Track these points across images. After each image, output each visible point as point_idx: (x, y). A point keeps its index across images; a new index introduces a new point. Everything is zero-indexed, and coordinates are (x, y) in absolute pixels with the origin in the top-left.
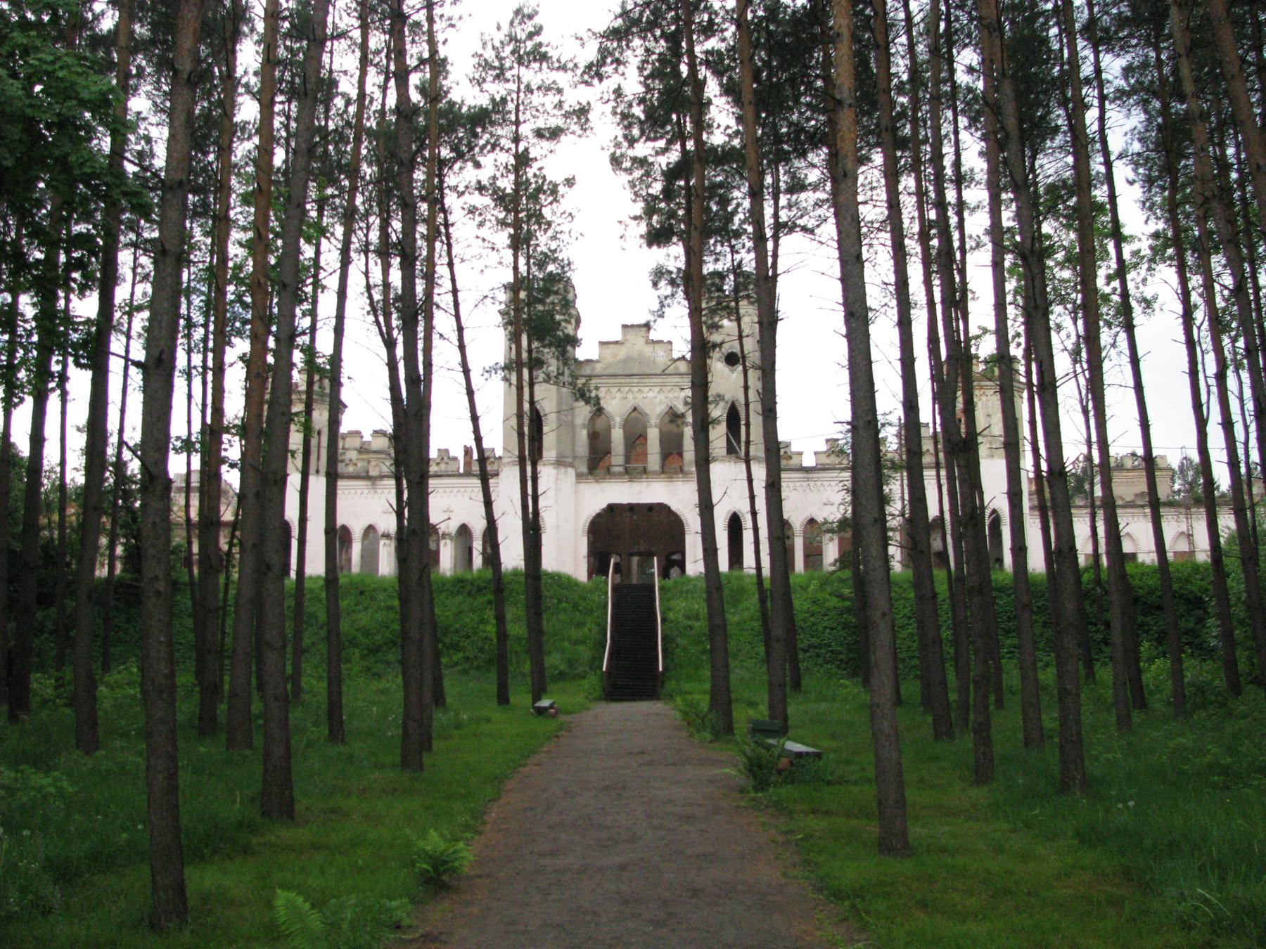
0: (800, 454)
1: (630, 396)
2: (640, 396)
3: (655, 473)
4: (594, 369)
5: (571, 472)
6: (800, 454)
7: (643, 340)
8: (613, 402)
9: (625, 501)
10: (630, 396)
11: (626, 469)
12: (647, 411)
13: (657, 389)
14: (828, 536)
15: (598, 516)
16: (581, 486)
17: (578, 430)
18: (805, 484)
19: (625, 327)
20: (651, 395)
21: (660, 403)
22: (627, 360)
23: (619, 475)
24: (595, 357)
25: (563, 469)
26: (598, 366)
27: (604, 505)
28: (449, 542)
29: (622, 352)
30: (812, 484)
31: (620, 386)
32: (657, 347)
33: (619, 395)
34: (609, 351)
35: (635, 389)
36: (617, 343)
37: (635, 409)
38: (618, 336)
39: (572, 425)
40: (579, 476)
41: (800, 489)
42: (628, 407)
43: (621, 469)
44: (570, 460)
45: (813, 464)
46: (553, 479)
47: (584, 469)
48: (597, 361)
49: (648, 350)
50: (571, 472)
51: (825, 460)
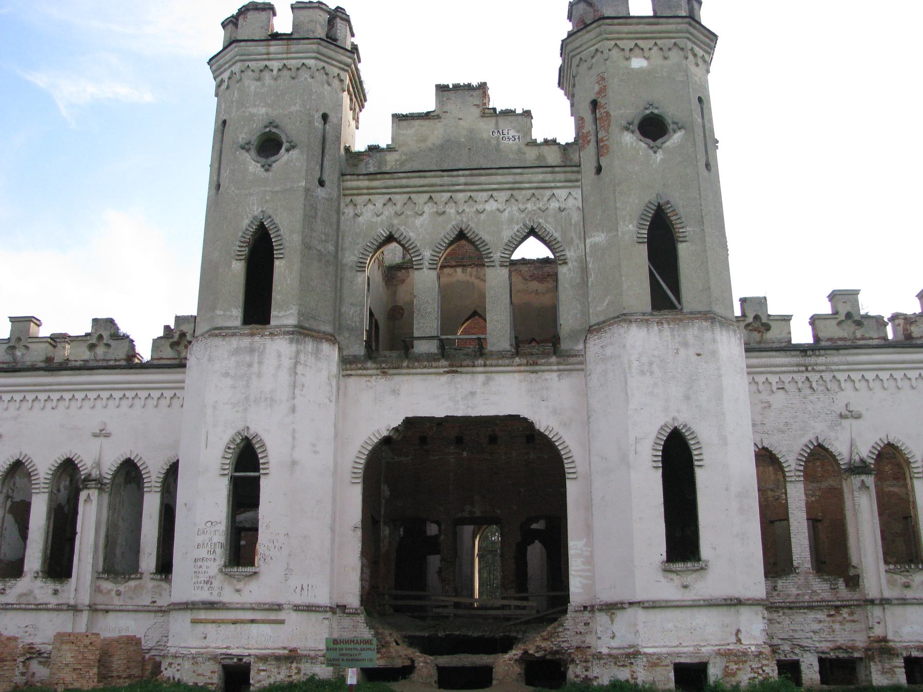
0: (787, 319)
1: (451, 210)
2: (469, 209)
3: (501, 355)
4: (382, 162)
5: (331, 353)
6: (786, 319)
7: (477, 112)
8: (418, 221)
9: (439, 412)
10: (451, 210)
11: (442, 344)
12: (486, 237)
13: (503, 196)
14: (856, 480)
15: (386, 441)
16: (352, 381)
17: (348, 274)
18: (800, 378)
19: (442, 89)
20: (491, 206)
21: (511, 220)
22: (446, 146)
23: (430, 359)
24: (384, 141)
25: (310, 345)
26: (391, 158)
27: (397, 421)
28: (94, 493)
29: (436, 133)
30: (814, 377)
31: (431, 193)
32: (503, 123)
33: (429, 209)
34: (412, 130)
35: (461, 196)
36: (427, 116)
37: (461, 235)
38: (428, 104)
39: (334, 263)
40: (348, 363)
41: (791, 387)
42: (447, 230)
43: (431, 347)
44: (328, 328)
45: (810, 340)
46: (287, 363)
47: (359, 350)
48: (390, 149)
49: (486, 128)
50: (331, 353)
51: (831, 331)
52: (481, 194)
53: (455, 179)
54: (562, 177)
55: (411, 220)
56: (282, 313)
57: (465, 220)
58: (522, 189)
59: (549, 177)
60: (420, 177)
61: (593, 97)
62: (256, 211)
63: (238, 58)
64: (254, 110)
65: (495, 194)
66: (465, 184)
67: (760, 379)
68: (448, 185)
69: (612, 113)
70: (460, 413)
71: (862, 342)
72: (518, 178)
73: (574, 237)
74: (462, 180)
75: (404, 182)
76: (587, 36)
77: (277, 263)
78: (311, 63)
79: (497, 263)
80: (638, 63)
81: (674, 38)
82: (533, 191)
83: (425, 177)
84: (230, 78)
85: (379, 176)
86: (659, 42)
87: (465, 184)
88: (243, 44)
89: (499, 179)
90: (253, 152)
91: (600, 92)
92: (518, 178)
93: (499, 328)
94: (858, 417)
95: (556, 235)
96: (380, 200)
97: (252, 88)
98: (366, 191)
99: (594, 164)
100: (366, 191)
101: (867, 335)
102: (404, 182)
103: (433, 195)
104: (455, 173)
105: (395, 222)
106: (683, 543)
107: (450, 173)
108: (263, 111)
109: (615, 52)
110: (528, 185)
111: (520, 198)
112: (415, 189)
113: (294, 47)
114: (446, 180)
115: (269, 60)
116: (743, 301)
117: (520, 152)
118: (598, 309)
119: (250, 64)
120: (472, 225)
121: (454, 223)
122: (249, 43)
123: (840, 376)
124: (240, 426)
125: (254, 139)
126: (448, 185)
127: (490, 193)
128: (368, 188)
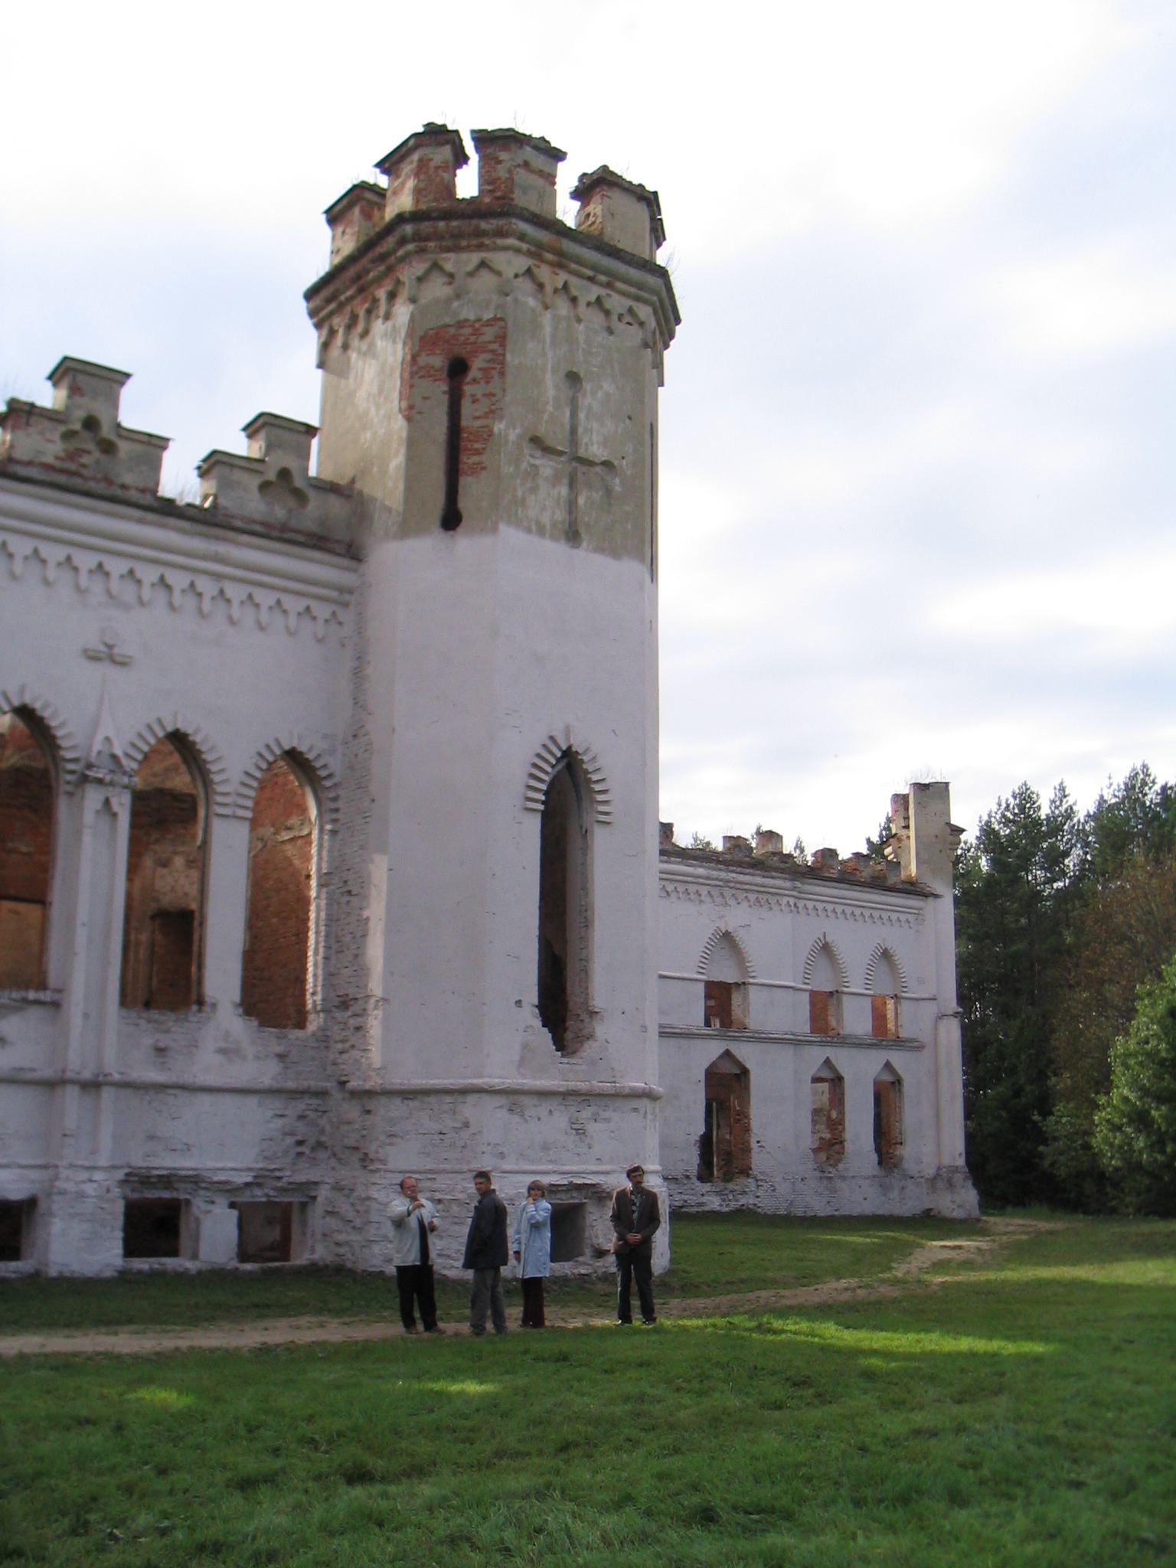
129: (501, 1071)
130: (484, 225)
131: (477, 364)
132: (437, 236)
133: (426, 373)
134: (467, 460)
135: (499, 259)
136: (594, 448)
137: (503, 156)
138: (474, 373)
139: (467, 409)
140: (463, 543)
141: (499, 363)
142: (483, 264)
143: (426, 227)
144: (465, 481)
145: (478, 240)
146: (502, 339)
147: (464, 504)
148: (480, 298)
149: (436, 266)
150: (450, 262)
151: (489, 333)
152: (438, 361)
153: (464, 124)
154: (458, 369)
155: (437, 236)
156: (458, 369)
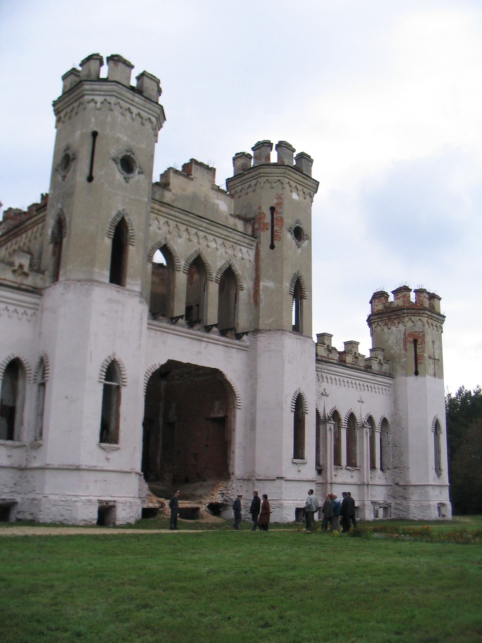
8: (180, 241)
21: (221, 257)
27: (164, 362)
33: (185, 235)
52: (210, 236)
53: (201, 223)
54: (247, 241)
55: (176, 238)
56: (132, 282)
57: (201, 249)
58: (228, 240)
59: (242, 239)
60: (185, 215)
61: (273, 205)
62: (120, 209)
63: (115, 94)
64: (120, 136)
65: (217, 239)
66: (206, 228)
67: (320, 374)
68: (197, 225)
69: (285, 220)
70: (193, 363)
71: (331, 361)
72: (229, 234)
73: (247, 277)
74: (205, 225)
75: (177, 214)
76: (276, 170)
77: (131, 247)
78: (154, 119)
79: (214, 280)
80: (295, 196)
81: (140, 109)
82: (233, 244)
83: (187, 216)
84: (102, 103)
85: (166, 206)
86: (305, 189)
87: (206, 228)
88: (120, 86)
89: (221, 231)
90: (119, 165)
91: (278, 204)
92: (229, 234)
93: (179, 308)
94: (327, 396)
95: (239, 272)
96: (162, 220)
97: (119, 119)
98: (156, 211)
99: (270, 243)
100: (156, 211)
101: (333, 358)
102: (177, 214)
103: (189, 228)
104: (203, 220)
105: (168, 237)
106: (298, 453)
107: (201, 219)
108: (125, 139)
109: (287, 185)
110: (232, 240)
111: (227, 245)
112: (181, 221)
113: (148, 105)
114: (197, 222)
115: (132, 105)
116: (319, 336)
117: (226, 218)
118: (266, 322)
119: (121, 102)
120: (204, 253)
121: (196, 248)
122: (124, 88)
123: (324, 375)
124: (110, 353)
125: (120, 156)
126: (197, 225)
127: (214, 237)
128: (158, 210)
129: (431, 482)
130: (420, 312)
131: (420, 341)
132: (411, 313)
133: (410, 342)
134: (419, 361)
135: (423, 318)
136: (437, 357)
137: (421, 295)
138: (419, 343)
139: (418, 351)
140: (420, 378)
141: (424, 340)
142: (419, 319)
143: (409, 311)
144: (419, 366)
145: (419, 315)
146: (424, 336)
147: (419, 370)
148: (418, 327)
149: (410, 319)
150: (413, 318)
151: (421, 334)
152: (411, 339)
153: (413, 286)
154: (415, 342)
155: (411, 313)
156: (415, 342)
